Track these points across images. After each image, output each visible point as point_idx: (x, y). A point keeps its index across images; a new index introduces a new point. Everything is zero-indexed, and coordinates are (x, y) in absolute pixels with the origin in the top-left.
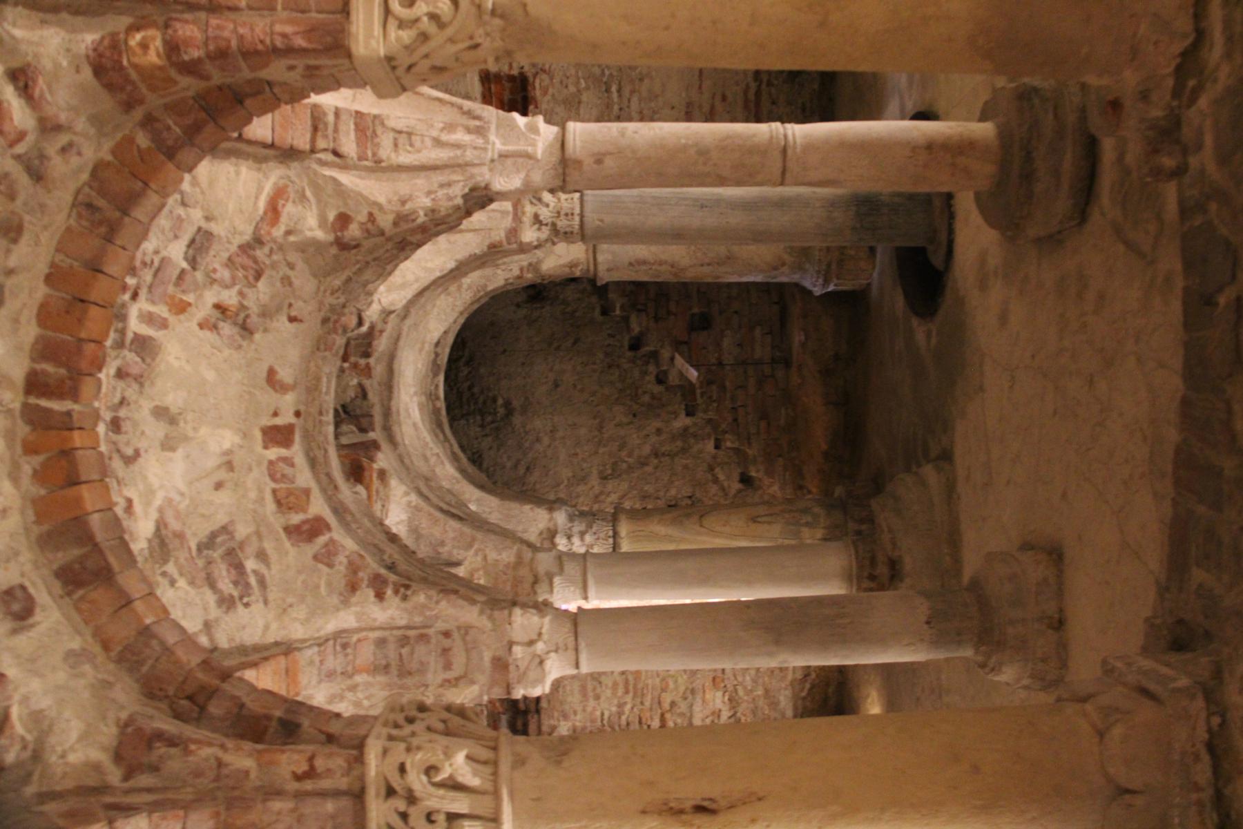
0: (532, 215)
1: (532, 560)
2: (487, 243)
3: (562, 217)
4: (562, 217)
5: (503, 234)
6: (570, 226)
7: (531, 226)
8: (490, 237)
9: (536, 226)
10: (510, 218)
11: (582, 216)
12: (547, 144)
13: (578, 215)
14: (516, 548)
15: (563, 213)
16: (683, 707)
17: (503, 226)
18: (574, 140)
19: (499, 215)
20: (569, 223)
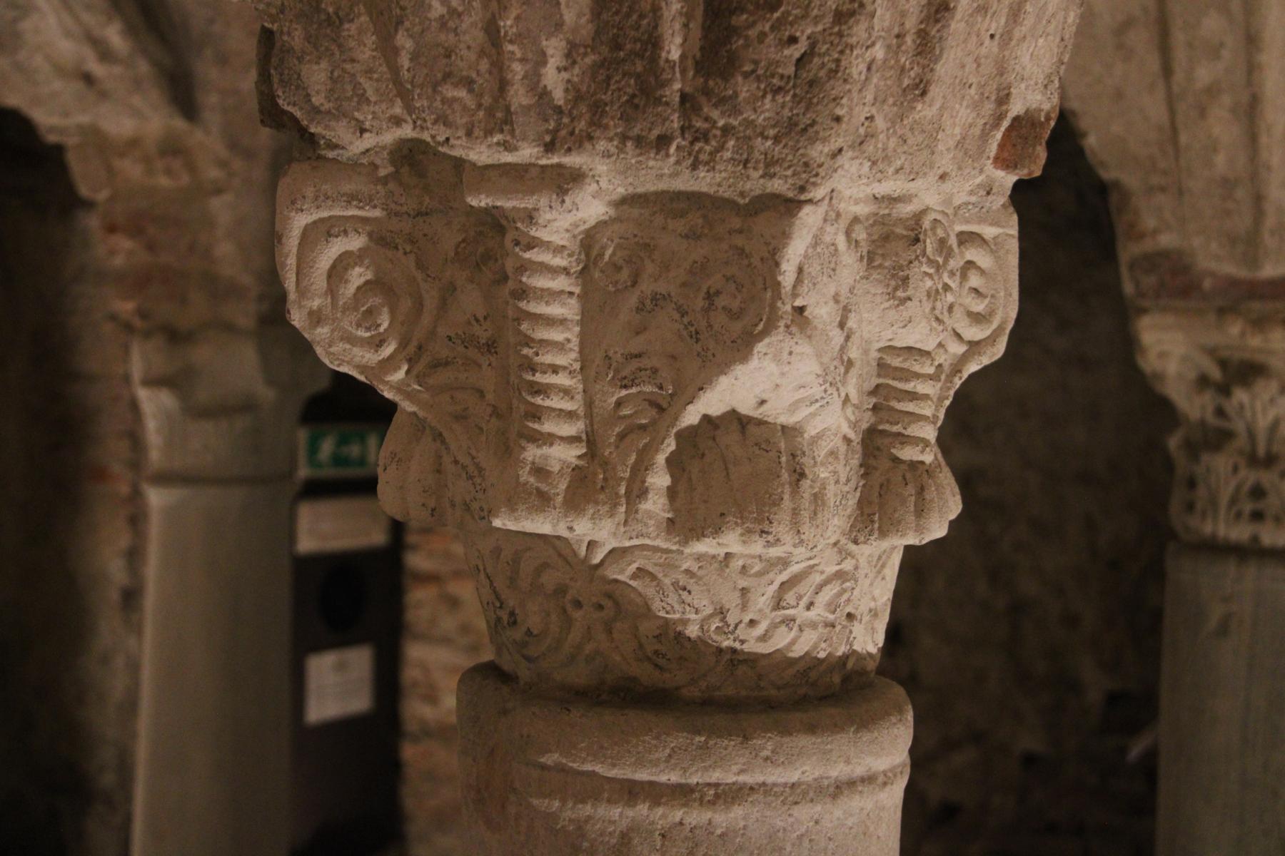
0: (1260, 358)
1: (229, 328)
2: (1131, 180)
3: (1250, 477)
4: (1250, 477)
5: (1167, 240)
6: (1213, 502)
7: (1212, 352)
8: (1151, 190)
9: (1216, 373)
10: (1230, 269)
11: (1250, 552)
12: (623, 573)
13: (1255, 539)
14: (247, 280)
15: (1267, 478)
16: (448, 623)
17: (1197, 242)
18: (632, 792)
19: (1242, 222)
20: (1224, 499)
